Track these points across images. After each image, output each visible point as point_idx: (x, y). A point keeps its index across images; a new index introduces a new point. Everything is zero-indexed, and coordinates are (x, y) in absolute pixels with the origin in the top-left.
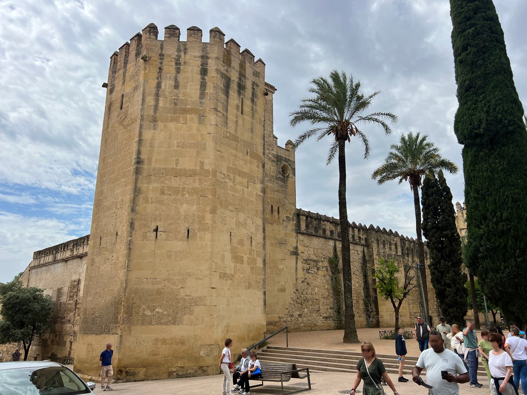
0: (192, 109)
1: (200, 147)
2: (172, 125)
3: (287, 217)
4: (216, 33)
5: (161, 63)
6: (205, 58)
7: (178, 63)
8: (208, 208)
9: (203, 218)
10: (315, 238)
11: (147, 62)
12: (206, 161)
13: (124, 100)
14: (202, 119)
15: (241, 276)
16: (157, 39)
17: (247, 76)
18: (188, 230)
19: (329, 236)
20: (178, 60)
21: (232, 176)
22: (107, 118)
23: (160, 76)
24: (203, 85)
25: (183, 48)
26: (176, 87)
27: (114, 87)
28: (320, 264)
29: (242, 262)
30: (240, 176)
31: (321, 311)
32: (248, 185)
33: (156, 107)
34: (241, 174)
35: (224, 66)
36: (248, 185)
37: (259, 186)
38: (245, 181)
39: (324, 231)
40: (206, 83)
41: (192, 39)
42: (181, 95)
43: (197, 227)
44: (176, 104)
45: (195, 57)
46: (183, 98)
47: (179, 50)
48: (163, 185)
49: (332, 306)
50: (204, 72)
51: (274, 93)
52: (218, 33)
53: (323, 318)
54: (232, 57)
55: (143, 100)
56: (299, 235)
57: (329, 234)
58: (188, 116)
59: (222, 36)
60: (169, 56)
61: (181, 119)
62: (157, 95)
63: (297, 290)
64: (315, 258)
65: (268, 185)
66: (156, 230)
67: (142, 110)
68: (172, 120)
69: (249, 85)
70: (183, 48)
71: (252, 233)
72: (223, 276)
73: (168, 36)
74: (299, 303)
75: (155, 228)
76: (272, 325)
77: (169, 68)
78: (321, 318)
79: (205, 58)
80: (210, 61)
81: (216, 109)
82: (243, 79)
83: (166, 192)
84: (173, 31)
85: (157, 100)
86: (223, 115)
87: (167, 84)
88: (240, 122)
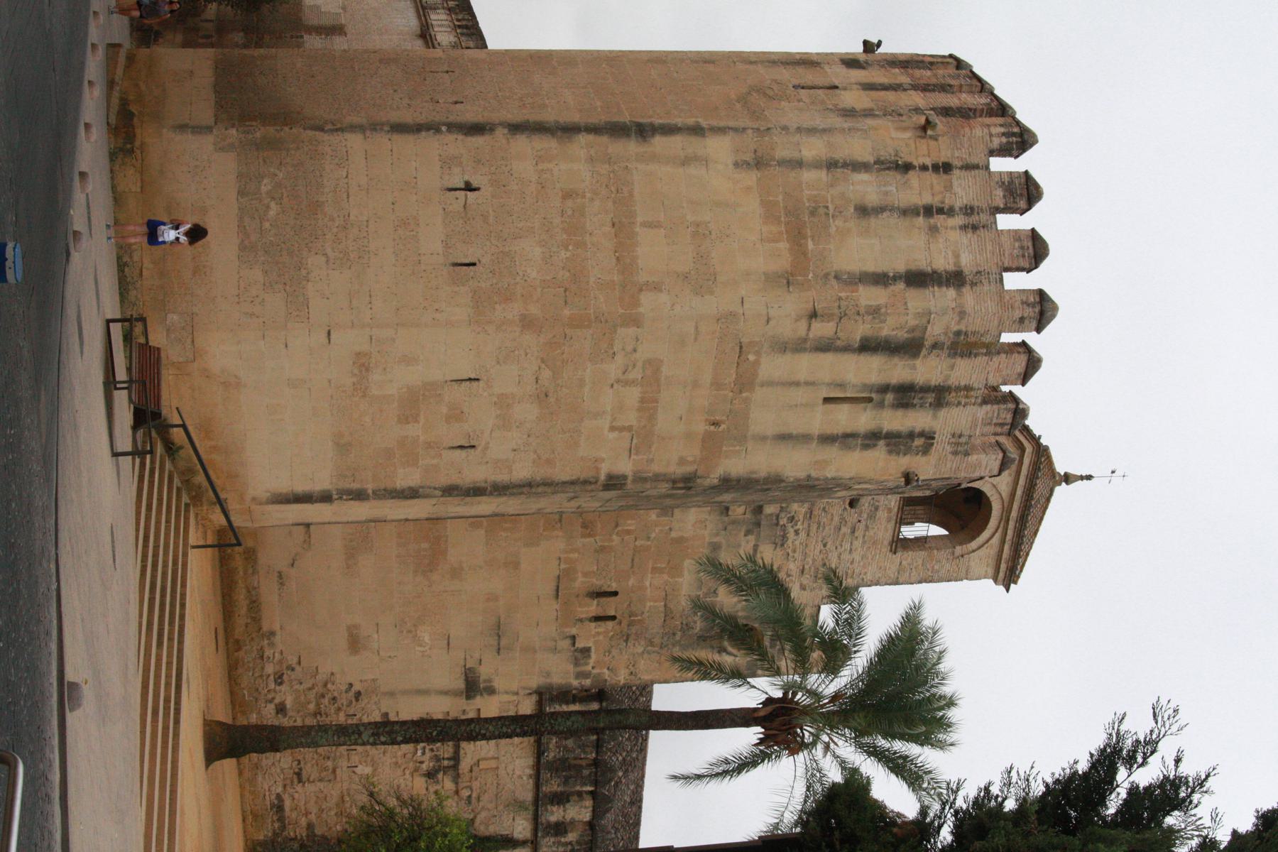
0: (805, 254)
1: (701, 279)
2: (752, 205)
3: (586, 651)
4: (1041, 310)
5: (924, 168)
6: (956, 279)
7: (928, 211)
8: (534, 310)
9: (508, 299)
10: (531, 761)
11: (920, 133)
12: (663, 297)
13: (820, 92)
14: (788, 280)
15: (367, 419)
16: (992, 153)
17: (943, 413)
18: (474, 264)
19: (543, 820)
20: (940, 211)
21: (635, 374)
22: (776, 58)
23: (888, 169)
24: (881, 279)
25: (976, 220)
26: (863, 211)
27: (864, 68)
28: (449, 785)
29: (405, 419)
30: (642, 400)
31: (299, 788)
32: (621, 429)
33: (799, 164)
34: (648, 405)
35: (946, 334)
36: (621, 429)
37: (625, 467)
38: (631, 418)
39: (560, 799)
40: (886, 285)
41: (1006, 242)
42: (839, 222)
43: (483, 285)
44: (813, 213)
45: (957, 256)
46: (833, 230)
47: (969, 210)
48: (588, 195)
49: (318, 831)
50: (918, 279)
51: (996, 581)
52: (1037, 310)
53: (278, 796)
54: (981, 360)
55: (812, 131)
56: (534, 698)
57: (553, 819)
58: (783, 245)
59: (1034, 324)
60: (949, 187)
61: (774, 229)
62: (832, 165)
63: (358, 695)
64: (465, 765)
65: (681, 575)
66: (469, 188)
67: (785, 128)
68: (768, 206)
69: (917, 419)
70: (976, 220)
71: (486, 448)
72: (362, 364)
73: (1006, 179)
74: (318, 704)
75: (475, 185)
76: (250, 609)
77: (918, 190)
78: (280, 790)
79: (956, 279)
80: (951, 293)
81: (814, 315)
82: (930, 398)
83: (569, 203)
84: (1025, 192)
85: (817, 165)
86: (805, 340)
87: (866, 187)
88: (799, 395)
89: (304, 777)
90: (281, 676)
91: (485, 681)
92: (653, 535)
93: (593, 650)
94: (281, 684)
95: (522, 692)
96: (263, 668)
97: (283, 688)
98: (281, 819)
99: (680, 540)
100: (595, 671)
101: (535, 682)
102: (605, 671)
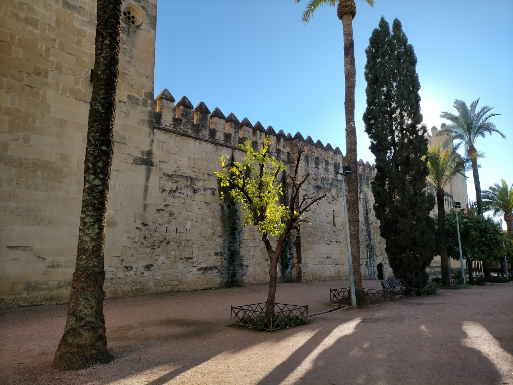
56: (156, 131)
89: (191, 256)
90: (126, 268)
91: (143, 155)
92: (52, 37)
93: (130, 93)
94: (131, 267)
95: (152, 137)
96: (119, 278)
97: (134, 266)
98: (211, 269)
99: (58, 22)
100: (143, 96)
101: (146, 129)
102: (143, 91)
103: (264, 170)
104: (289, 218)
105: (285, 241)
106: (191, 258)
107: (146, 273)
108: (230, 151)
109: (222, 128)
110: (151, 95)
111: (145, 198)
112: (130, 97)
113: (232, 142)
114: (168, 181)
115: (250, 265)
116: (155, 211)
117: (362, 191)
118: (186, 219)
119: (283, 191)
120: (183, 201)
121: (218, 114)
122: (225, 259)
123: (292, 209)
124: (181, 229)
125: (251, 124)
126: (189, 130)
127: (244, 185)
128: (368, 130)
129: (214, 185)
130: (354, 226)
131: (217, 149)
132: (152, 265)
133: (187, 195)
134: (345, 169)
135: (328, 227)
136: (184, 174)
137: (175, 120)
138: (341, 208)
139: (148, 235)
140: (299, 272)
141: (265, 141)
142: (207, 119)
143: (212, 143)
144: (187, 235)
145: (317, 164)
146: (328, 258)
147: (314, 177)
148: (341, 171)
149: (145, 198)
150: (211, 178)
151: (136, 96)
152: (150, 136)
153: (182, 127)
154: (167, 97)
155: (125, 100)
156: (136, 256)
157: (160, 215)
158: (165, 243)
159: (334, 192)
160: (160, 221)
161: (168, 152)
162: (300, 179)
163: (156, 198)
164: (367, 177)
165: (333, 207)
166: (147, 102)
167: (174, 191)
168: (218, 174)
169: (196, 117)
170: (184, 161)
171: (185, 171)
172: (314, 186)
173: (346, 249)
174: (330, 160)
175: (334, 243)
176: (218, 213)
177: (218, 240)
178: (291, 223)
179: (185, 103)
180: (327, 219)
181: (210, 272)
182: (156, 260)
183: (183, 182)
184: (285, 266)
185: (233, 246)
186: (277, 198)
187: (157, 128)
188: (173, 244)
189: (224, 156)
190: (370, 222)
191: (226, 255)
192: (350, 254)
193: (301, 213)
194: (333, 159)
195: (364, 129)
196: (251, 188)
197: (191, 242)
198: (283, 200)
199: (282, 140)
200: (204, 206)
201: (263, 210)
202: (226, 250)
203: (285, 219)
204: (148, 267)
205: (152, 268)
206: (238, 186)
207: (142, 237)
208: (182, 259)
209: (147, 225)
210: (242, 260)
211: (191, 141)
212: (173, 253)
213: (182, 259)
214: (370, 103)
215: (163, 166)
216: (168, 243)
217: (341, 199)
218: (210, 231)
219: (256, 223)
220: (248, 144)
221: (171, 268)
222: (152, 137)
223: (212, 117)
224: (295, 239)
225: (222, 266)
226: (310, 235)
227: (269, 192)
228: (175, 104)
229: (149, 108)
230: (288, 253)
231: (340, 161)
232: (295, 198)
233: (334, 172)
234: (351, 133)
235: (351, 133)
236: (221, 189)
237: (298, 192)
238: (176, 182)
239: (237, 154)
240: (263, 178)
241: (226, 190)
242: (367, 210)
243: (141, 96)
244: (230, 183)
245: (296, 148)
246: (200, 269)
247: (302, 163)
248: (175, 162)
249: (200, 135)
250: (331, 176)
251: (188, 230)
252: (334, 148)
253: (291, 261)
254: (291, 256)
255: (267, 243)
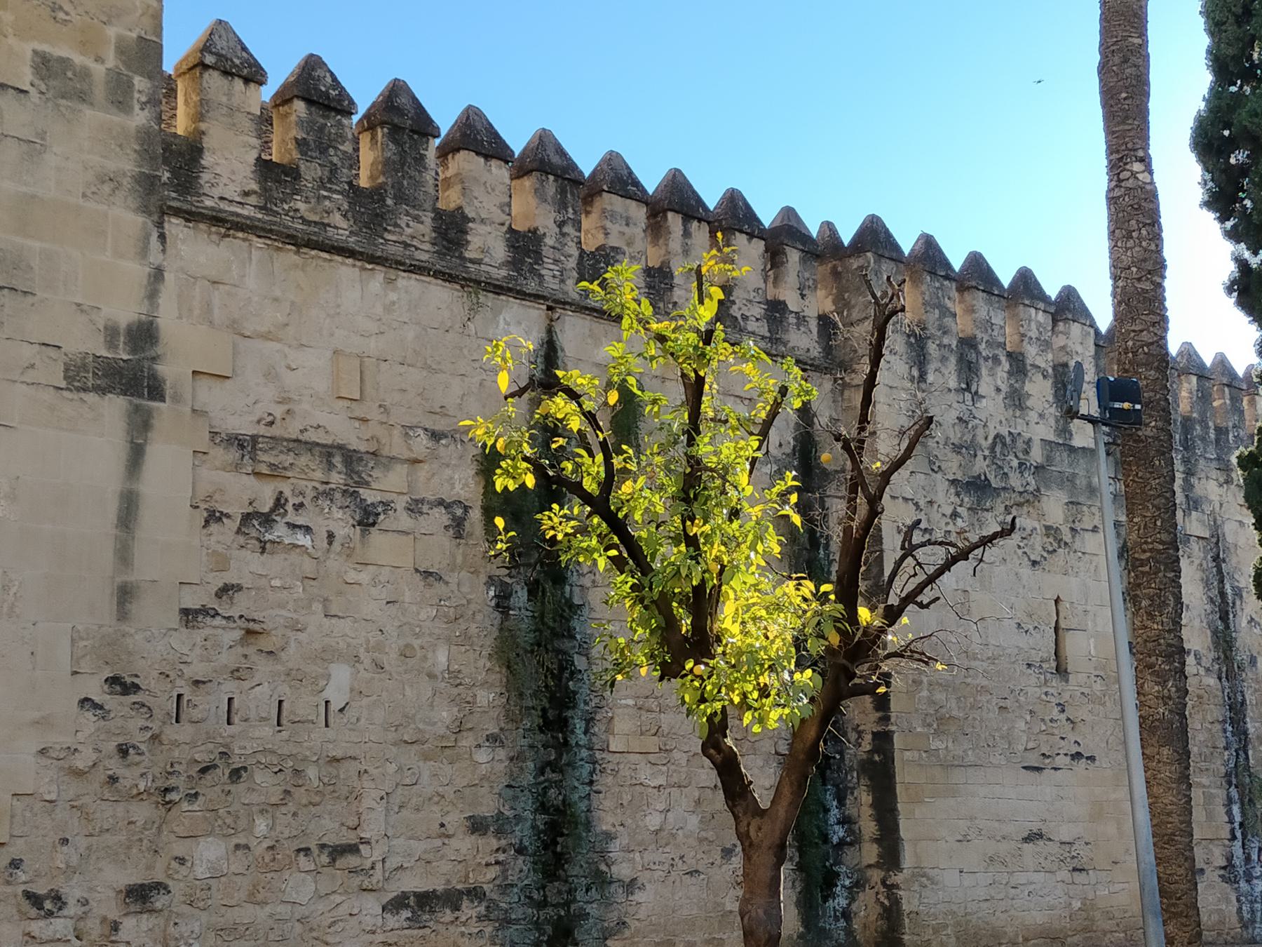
56: (174, 226)
91: (111, 344)
95: (155, 257)
100: (111, 61)
101: (128, 219)
103: (707, 408)
104: (835, 639)
105: (814, 758)
106: (352, 849)
107: (128, 924)
108: (535, 314)
109: (495, 205)
110: (146, 52)
111: (124, 556)
112: (45, 65)
113: (548, 270)
114: (237, 467)
115: (643, 877)
116: (174, 619)
117: (1194, 504)
118: (326, 655)
119: (801, 508)
120: (308, 566)
121: (476, 136)
122: (521, 851)
123: (848, 597)
124: (302, 705)
125: (637, 183)
126: (337, 219)
127: (608, 484)
128: (1222, 200)
129: (462, 483)
130: (1162, 679)
131: (475, 309)
132: (159, 887)
133: (331, 536)
134: (1109, 391)
135: (1031, 684)
136: (311, 436)
137: (265, 168)
138: (1092, 585)
139: (140, 739)
140: (892, 913)
141: (709, 264)
142: (421, 159)
143: (449, 278)
144: (330, 733)
145: (968, 370)
146: (1033, 837)
147: (955, 435)
148: (1089, 404)
149: (124, 556)
150: (447, 450)
151: (78, 59)
152: (144, 252)
153: (301, 206)
154: (225, 59)
155: (25, 77)
156: (82, 843)
157: (198, 636)
158: (222, 773)
159: (1054, 506)
160: (198, 670)
161: (235, 328)
162: (885, 446)
163: (174, 551)
164: (1221, 431)
165: (1051, 582)
166: (130, 85)
167: (267, 520)
168: (482, 432)
169: (368, 156)
170: (310, 371)
171: (321, 417)
172: (954, 482)
173: (1123, 793)
174: (1031, 351)
175: (1062, 761)
176: (483, 623)
177: (482, 756)
178: (846, 665)
179: (315, 89)
180: (1023, 641)
181: (448, 915)
182: (181, 861)
183: (309, 474)
184: (819, 884)
185: (558, 785)
186: (773, 543)
187: (177, 212)
188: (261, 778)
189: (512, 336)
190: (1241, 656)
191: (522, 833)
192: (1143, 816)
193: (892, 615)
194: (1046, 345)
195: (1199, 194)
196: (645, 498)
197: (353, 767)
198: (803, 555)
199: (793, 256)
200: (411, 590)
201: (704, 601)
202: (526, 804)
203: (815, 647)
204: (140, 895)
205: (160, 901)
206: (577, 488)
207: (111, 746)
208: (307, 851)
209: (136, 688)
210: (603, 854)
211: (346, 270)
212: (261, 826)
213: (307, 851)
214: (1228, 64)
215: (211, 396)
216: (236, 774)
217: (1091, 543)
218: (446, 714)
219: (670, 671)
220: (626, 279)
221: (252, 899)
222: (155, 257)
223: (447, 151)
224: (867, 745)
225: (505, 888)
226: (942, 723)
227: (734, 514)
228: (267, 93)
229: (140, 118)
230: (834, 813)
231: (1082, 351)
232: (861, 541)
233: (1053, 411)
234: (1134, 217)
235: (1134, 217)
236: (495, 503)
237: (874, 511)
238: (276, 473)
239: (572, 330)
240: (703, 448)
241: (519, 508)
242: (1222, 594)
243: (99, 59)
244: (539, 471)
245: (865, 292)
246: (398, 904)
247: (894, 368)
248: (270, 375)
249: (390, 244)
250: (1039, 427)
251: (334, 707)
252: (1052, 291)
253: (849, 856)
254: (850, 832)
255: (728, 768)
